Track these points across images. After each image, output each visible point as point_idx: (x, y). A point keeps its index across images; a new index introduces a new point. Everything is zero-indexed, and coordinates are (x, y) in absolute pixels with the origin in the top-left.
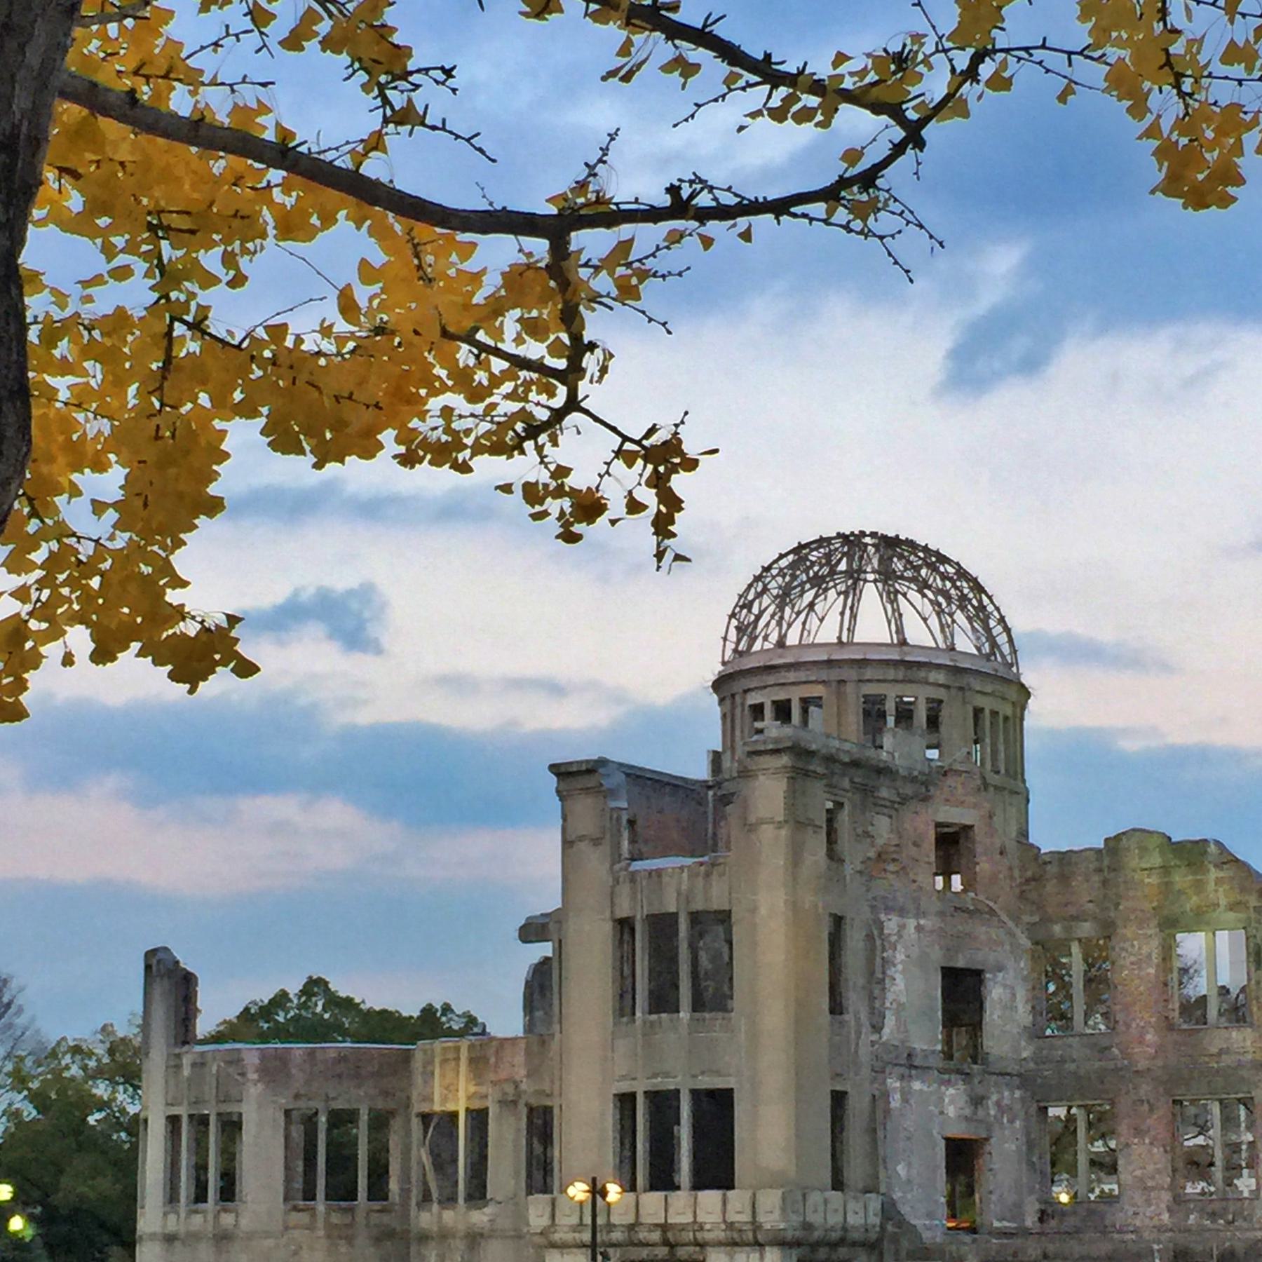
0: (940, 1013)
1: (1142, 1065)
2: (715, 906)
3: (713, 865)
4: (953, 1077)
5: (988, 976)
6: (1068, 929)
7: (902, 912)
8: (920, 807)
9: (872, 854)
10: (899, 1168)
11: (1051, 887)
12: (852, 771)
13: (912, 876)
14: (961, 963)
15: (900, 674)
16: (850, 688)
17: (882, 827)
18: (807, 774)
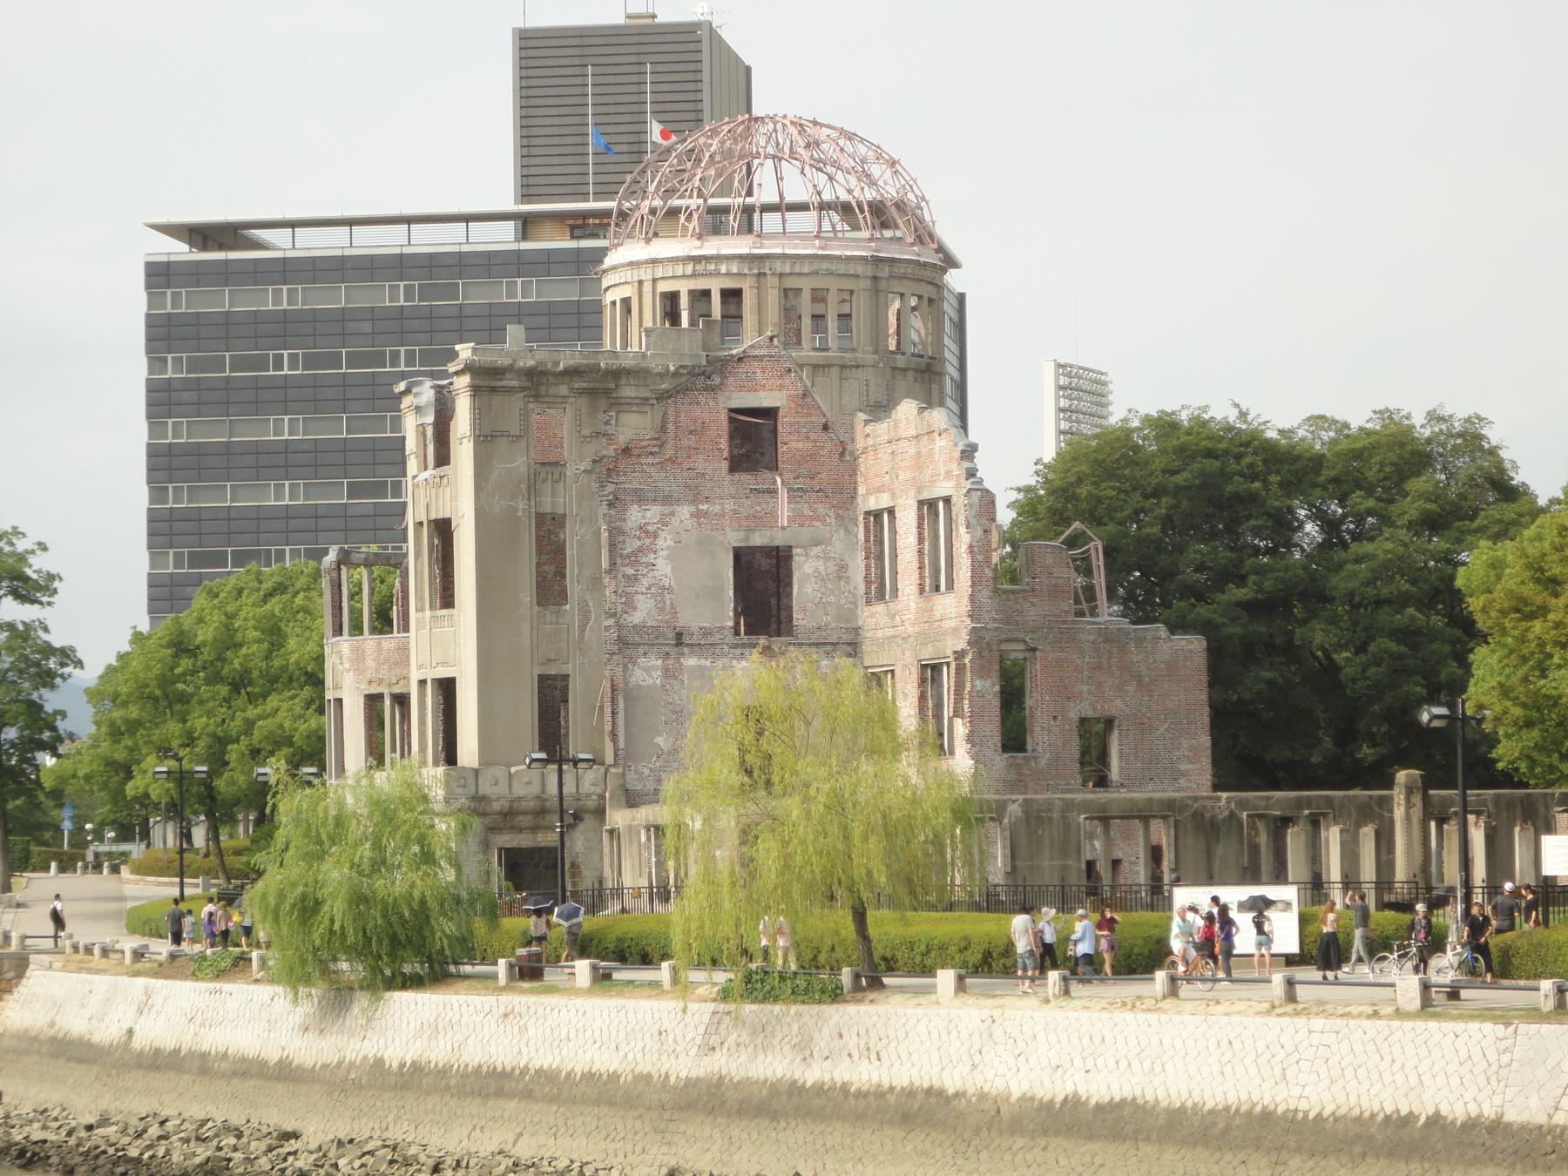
0: (731, 593)
1: (910, 630)
2: (441, 516)
3: (441, 477)
4: (747, 651)
5: (795, 551)
6: (877, 499)
7: (667, 500)
8: (702, 399)
9: (610, 451)
10: (659, 740)
11: (871, 455)
12: (567, 379)
13: (686, 466)
14: (758, 540)
15: (689, 269)
16: (647, 287)
17: (633, 426)
18: (493, 390)
